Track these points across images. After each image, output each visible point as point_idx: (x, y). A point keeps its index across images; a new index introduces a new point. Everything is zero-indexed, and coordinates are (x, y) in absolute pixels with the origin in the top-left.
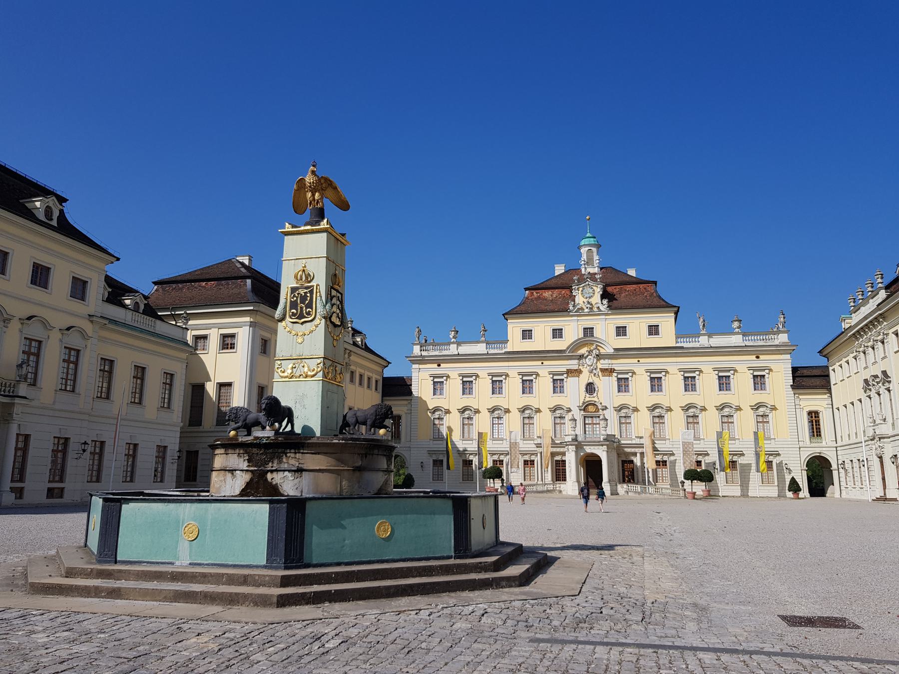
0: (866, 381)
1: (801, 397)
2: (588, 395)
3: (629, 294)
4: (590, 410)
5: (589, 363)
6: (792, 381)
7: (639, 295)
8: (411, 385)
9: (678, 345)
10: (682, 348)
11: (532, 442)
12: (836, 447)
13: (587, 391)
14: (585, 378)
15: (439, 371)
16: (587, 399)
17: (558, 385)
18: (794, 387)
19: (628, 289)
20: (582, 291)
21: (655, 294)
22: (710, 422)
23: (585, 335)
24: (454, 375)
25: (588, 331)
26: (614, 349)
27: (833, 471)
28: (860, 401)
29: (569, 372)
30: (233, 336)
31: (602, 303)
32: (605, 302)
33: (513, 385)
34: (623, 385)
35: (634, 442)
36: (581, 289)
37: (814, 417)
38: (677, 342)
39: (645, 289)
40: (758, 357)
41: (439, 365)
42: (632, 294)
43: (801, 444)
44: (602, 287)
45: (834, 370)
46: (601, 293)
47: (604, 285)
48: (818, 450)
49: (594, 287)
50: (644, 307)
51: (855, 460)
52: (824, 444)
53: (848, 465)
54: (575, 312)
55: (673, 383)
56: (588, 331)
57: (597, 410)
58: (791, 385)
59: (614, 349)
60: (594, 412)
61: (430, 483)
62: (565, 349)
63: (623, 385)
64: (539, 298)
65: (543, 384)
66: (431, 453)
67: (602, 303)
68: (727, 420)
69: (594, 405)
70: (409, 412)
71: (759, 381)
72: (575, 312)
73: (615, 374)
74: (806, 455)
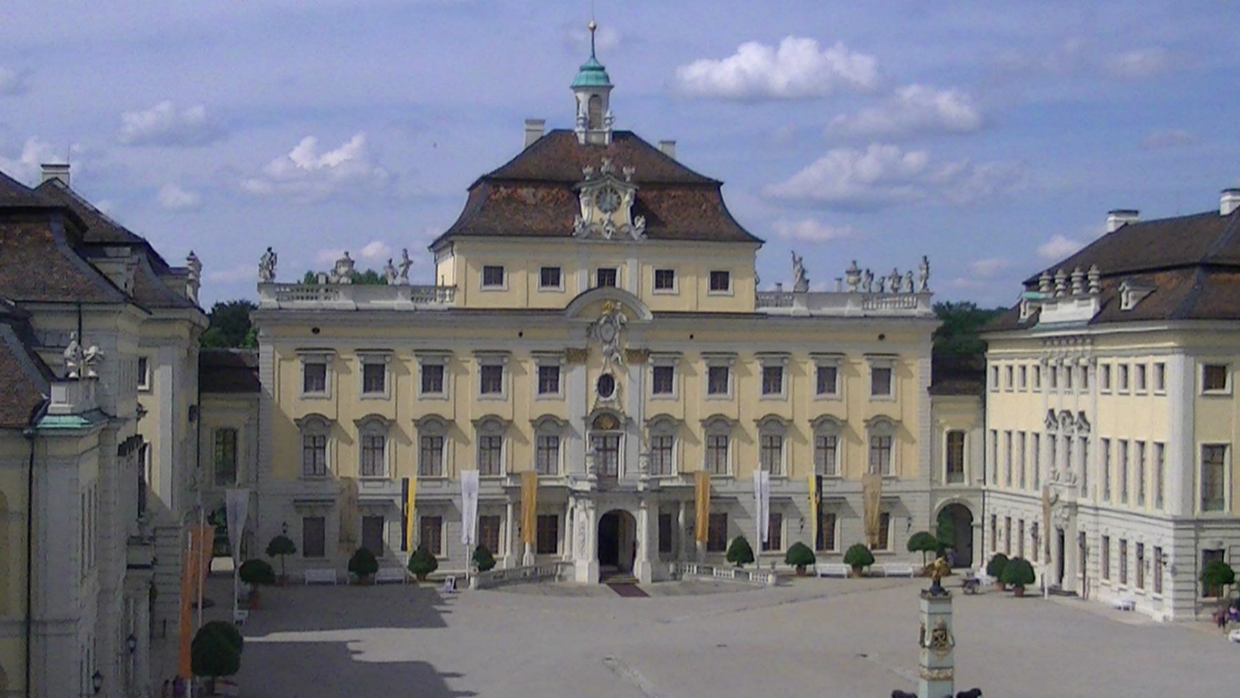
0: (1052, 412)
1: (940, 406)
2: (602, 399)
3: (676, 204)
6: (930, 381)
7: (693, 206)
8: (257, 369)
9: (762, 310)
10: (764, 315)
11: (498, 483)
12: (984, 491)
13: (600, 392)
15: (316, 342)
17: (549, 379)
18: (932, 390)
19: (673, 194)
20: (598, 197)
21: (720, 208)
23: (601, 283)
26: (653, 312)
27: (974, 529)
28: (1037, 436)
31: (633, 223)
32: (640, 222)
34: (663, 379)
35: (675, 483)
36: (596, 193)
37: (956, 439)
38: (757, 306)
39: (703, 195)
41: (316, 331)
42: (680, 204)
43: (936, 486)
44: (634, 192)
45: (996, 368)
46: (632, 203)
47: (636, 190)
48: (957, 496)
49: (622, 194)
50: (706, 238)
51: (1015, 521)
52: (966, 483)
53: (1001, 524)
54: (587, 238)
56: (607, 277)
57: (617, 425)
58: (929, 388)
59: (653, 312)
60: (612, 428)
62: (564, 306)
63: (663, 379)
64: (509, 199)
66: (298, 504)
67: (633, 223)
68: (826, 446)
72: (587, 238)
73: (650, 360)
74: (941, 502)
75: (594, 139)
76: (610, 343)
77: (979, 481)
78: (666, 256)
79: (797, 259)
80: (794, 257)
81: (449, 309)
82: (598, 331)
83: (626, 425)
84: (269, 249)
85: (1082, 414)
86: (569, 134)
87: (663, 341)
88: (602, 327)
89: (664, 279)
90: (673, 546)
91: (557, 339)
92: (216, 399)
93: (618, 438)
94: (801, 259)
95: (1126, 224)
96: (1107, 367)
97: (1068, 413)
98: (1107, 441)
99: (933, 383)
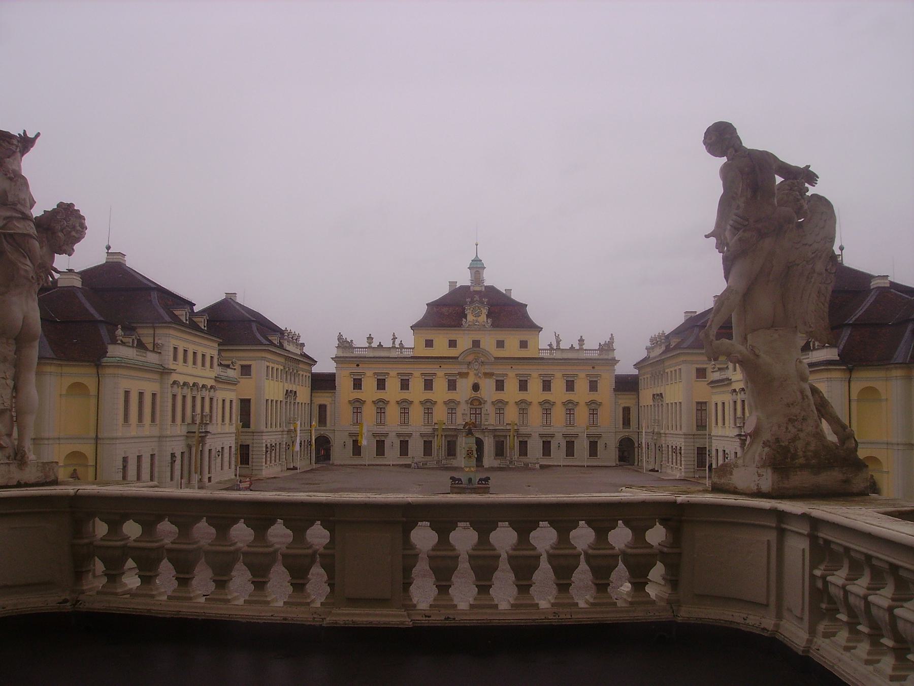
0: (654, 395)
2: (474, 393)
4: (476, 403)
5: (476, 367)
10: (542, 359)
12: (638, 432)
13: (473, 389)
14: (471, 380)
16: (473, 396)
17: (452, 385)
22: (558, 414)
24: (369, 373)
25: (476, 343)
29: (461, 375)
30: (250, 366)
33: (417, 384)
34: (500, 386)
36: (472, 309)
40: (593, 368)
41: (358, 365)
43: (617, 430)
45: (641, 380)
46: (487, 313)
49: (482, 309)
54: (467, 328)
55: (535, 385)
56: (476, 343)
57: (480, 404)
61: (351, 457)
63: (500, 386)
65: (440, 384)
66: (351, 435)
67: (487, 321)
69: (477, 399)
70: (334, 402)
71: (593, 386)
72: (467, 328)
74: (619, 436)
75: (478, 288)
76: (477, 370)
77: (636, 428)
78: (501, 335)
79: (557, 335)
80: (555, 334)
81: (412, 357)
82: (472, 365)
83: (484, 403)
84: (340, 333)
85: (661, 394)
86: (468, 287)
87: (498, 370)
88: (473, 364)
89: (500, 344)
90: (505, 455)
91: (454, 369)
92: (317, 393)
93: (481, 409)
94: (558, 335)
95: (691, 316)
96: (667, 373)
97: (658, 395)
98: (668, 404)
99: (616, 386)
